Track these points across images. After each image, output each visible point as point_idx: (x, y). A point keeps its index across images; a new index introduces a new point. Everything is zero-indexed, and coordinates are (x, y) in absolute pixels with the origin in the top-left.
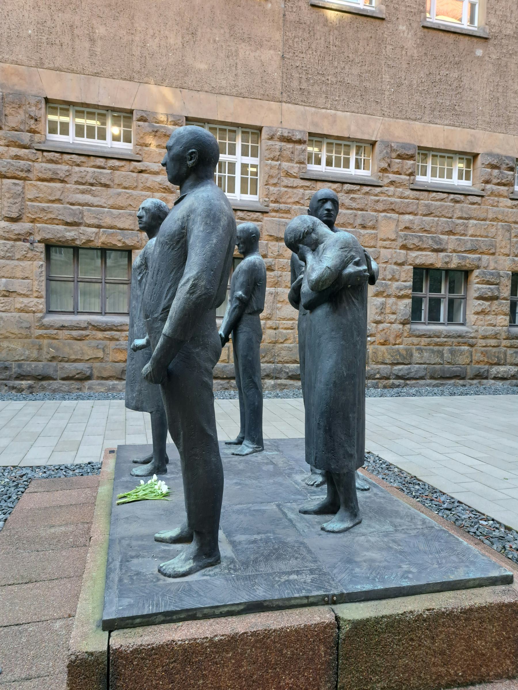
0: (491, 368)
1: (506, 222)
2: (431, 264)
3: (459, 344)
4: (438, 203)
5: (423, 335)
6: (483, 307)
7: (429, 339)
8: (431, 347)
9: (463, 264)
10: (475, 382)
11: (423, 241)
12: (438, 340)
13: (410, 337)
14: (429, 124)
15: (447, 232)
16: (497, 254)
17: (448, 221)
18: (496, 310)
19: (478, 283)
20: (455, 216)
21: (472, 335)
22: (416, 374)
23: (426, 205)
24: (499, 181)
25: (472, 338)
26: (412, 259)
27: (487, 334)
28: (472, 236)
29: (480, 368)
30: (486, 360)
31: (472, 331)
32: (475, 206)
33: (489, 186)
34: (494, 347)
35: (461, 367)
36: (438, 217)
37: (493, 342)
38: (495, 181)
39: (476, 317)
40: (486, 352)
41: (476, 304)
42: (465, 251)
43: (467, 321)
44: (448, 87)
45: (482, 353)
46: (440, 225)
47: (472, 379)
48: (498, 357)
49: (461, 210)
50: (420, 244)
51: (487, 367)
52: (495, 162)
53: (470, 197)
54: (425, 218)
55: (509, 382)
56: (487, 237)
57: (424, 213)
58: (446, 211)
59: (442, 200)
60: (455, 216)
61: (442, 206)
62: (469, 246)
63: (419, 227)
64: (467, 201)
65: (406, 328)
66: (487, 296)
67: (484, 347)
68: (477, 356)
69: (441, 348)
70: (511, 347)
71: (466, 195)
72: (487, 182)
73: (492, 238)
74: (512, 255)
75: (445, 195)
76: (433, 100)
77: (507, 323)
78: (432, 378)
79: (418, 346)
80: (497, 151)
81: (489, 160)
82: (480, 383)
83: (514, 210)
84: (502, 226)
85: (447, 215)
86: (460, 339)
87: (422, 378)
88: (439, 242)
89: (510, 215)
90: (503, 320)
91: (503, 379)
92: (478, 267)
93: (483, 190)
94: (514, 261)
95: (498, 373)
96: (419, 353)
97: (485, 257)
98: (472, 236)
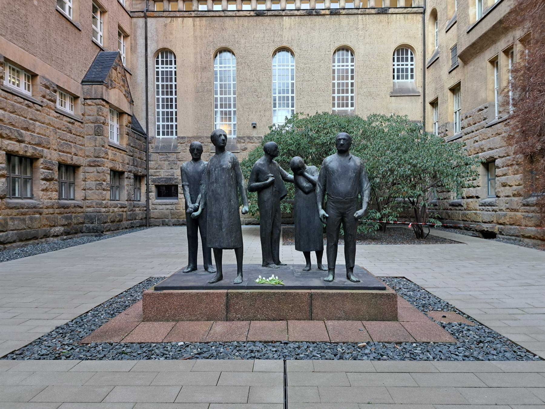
0: (51, 229)
1: (54, 127)
2: (17, 152)
3: (35, 213)
4: (18, 105)
5: (14, 207)
6: (47, 186)
7: (18, 210)
8: (19, 216)
9: (35, 153)
10: (43, 240)
11: (12, 133)
12: (23, 210)
13: (6, 209)
14: (10, 42)
15: (25, 128)
16: (51, 148)
17: (25, 120)
18: (53, 188)
19: (42, 168)
20: (28, 117)
21: (41, 206)
22: (11, 239)
23: (12, 105)
24: (50, 98)
25: (41, 208)
26: (6, 146)
27: (49, 205)
28: (38, 133)
29: (46, 230)
30: (49, 224)
31: (40, 203)
32: (38, 112)
33: (45, 100)
34: (52, 214)
35: (36, 230)
36: (19, 115)
37: (51, 211)
38: (48, 97)
39: (42, 193)
40: (48, 217)
41: (43, 183)
42: (35, 144)
43: (35, 195)
44: (20, 19)
45: (46, 219)
46: (21, 122)
47: (41, 238)
48: (54, 221)
49: (32, 114)
50: (10, 134)
51: (49, 228)
52: (48, 84)
53: (36, 105)
54: (11, 115)
55: (59, 238)
56: (45, 136)
57: (11, 110)
58: (23, 112)
59: (20, 103)
60: (28, 117)
61: (21, 108)
62: (37, 141)
63: (9, 121)
64: (34, 108)
65: (3, 202)
66: (48, 178)
67: (47, 214)
68: (45, 222)
69: (24, 217)
70: (60, 213)
71: (34, 103)
72: (44, 97)
73: (48, 137)
74: (58, 150)
75: (22, 100)
76: (12, 24)
77: (57, 197)
78: (21, 241)
79: (11, 216)
80: (47, 76)
81: (45, 82)
82: (46, 240)
83: (57, 120)
84: (53, 129)
85: (24, 116)
86: (34, 210)
87: (14, 242)
88: (21, 135)
89: (56, 123)
90: (55, 195)
91: (57, 236)
92: (42, 157)
93: (42, 102)
94: (59, 154)
95: (55, 232)
96: (12, 222)
97: (45, 150)
98: (38, 133)
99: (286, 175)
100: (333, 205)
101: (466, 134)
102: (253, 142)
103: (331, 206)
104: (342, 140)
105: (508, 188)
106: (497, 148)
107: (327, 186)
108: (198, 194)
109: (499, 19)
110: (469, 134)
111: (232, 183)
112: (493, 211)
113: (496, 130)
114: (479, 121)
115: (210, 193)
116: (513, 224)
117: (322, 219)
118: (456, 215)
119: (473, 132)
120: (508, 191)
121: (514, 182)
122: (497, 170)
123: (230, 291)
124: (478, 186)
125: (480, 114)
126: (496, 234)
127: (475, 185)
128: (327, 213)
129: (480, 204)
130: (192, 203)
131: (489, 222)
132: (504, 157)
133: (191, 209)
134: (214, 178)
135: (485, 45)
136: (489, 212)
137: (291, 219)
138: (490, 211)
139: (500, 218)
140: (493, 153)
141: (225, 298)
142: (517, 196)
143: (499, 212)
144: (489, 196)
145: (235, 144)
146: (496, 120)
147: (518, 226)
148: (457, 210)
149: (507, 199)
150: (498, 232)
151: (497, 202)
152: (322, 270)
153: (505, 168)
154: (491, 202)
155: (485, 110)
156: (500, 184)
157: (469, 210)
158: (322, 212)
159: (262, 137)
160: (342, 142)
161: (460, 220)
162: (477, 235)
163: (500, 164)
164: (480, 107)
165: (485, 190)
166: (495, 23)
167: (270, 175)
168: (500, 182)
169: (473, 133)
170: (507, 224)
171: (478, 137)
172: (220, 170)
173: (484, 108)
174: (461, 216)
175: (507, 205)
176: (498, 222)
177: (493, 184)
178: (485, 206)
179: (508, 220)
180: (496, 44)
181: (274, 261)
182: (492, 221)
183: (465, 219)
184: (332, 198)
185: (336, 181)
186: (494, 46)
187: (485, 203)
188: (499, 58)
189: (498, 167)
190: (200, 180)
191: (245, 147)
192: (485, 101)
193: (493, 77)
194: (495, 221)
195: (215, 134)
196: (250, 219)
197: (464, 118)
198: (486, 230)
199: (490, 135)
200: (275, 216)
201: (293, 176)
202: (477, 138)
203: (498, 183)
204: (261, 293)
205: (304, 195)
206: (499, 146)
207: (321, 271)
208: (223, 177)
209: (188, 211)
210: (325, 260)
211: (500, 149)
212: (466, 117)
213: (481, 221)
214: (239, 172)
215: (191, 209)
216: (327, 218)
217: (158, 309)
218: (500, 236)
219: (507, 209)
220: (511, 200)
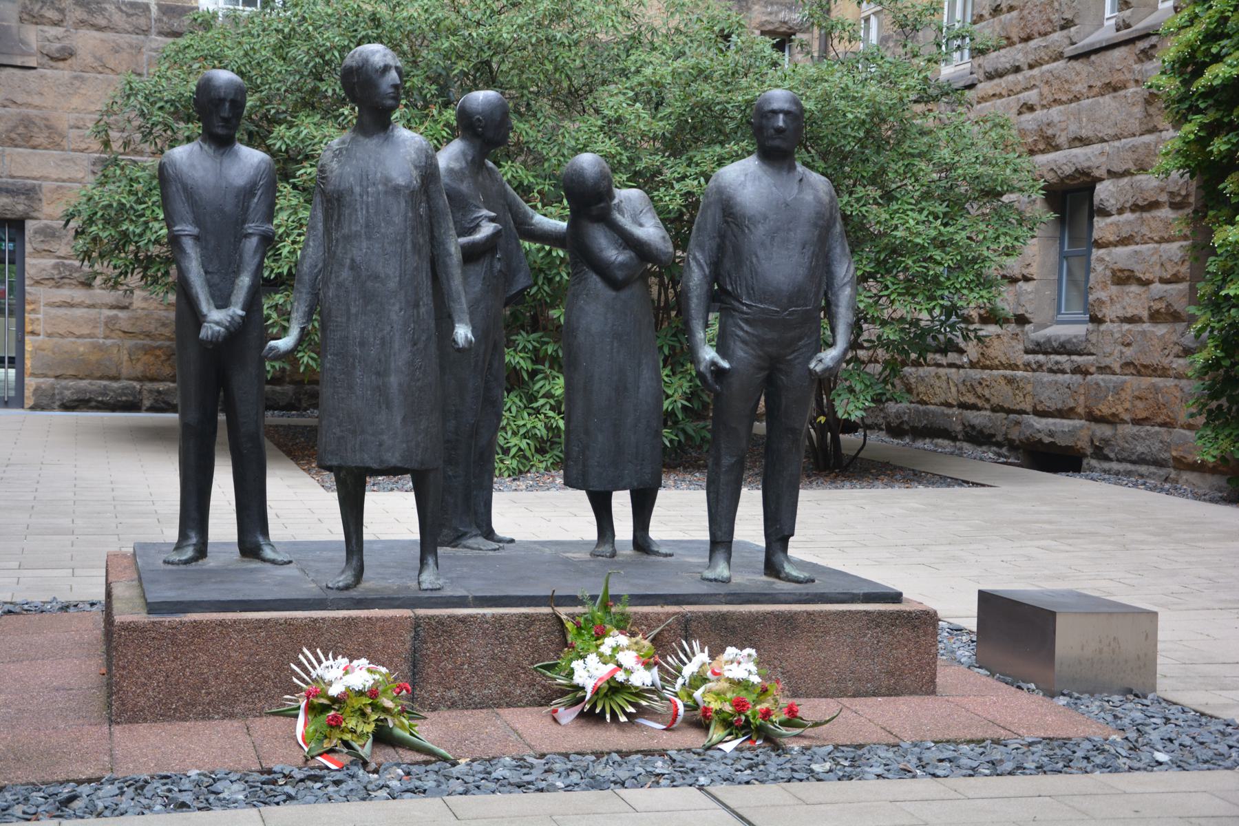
99: (525, 214)
101: (990, 77)
102: (103, 23)
103: (741, 333)
104: (781, 116)
105: (1134, 288)
106: (1103, 141)
107: (728, 264)
108: (237, 273)
110: (1001, 75)
111: (421, 241)
113: (1106, 70)
114: (1042, 29)
115: (345, 274)
116: (1146, 419)
117: (709, 376)
118: (938, 383)
119: (1017, 69)
120: (1134, 300)
121: (1157, 268)
122: (1099, 222)
123: (421, 612)
124: (1027, 279)
126: (1085, 456)
127: (1017, 272)
128: (724, 356)
130: (218, 307)
132: (1126, 173)
133: (217, 328)
134: (362, 221)
136: (1060, 377)
137: (278, 388)
138: (1063, 372)
140: (1089, 159)
141: (408, 637)
142: (1165, 321)
143: (1099, 377)
145: (14, 23)
146: (1107, 32)
147: (1161, 425)
148: (939, 365)
149: (1129, 331)
150: (1089, 451)
151: (1093, 338)
152: (657, 553)
153: (1128, 216)
154: (1069, 341)
156: (1108, 273)
157: (984, 367)
158: (708, 354)
159: (146, 8)
160: (781, 124)
161: (950, 405)
163: (1113, 201)
165: (1049, 292)
167: (485, 212)
168: (1107, 267)
169: (1020, 76)
170: (1123, 422)
171: (1035, 91)
172: (386, 193)
174: (954, 389)
175: (1128, 352)
177: (1079, 274)
178: (1046, 353)
179: (1127, 405)
181: (479, 527)
182: (1072, 409)
183: (970, 399)
185: (761, 253)
187: (1049, 340)
189: (1105, 213)
190: (244, 222)
191: (66, 43)
194: (1080, 410)
195: (367, 61)
196: (84, 384)
197: (986, 13)
198: (1047, 440)
199: (1080, 87)
200: (490, 364)
201: (564, 225)
202: (1032, 96)
203: (1100, 268)
204: (526, 616)
205: (610, 293)
206: (1111, 132)
207: (653, 558)
208: (396, 220)
209: (206, 332)
210: (624, 528)
211: (1117, 143)
212: (996, 11)
213: (1029, 408)
214: (441, 203)
215: (217, 328)
216: (719, 372)
217: (173, 680)
219: (1128, 364)
220: (1144, 333)
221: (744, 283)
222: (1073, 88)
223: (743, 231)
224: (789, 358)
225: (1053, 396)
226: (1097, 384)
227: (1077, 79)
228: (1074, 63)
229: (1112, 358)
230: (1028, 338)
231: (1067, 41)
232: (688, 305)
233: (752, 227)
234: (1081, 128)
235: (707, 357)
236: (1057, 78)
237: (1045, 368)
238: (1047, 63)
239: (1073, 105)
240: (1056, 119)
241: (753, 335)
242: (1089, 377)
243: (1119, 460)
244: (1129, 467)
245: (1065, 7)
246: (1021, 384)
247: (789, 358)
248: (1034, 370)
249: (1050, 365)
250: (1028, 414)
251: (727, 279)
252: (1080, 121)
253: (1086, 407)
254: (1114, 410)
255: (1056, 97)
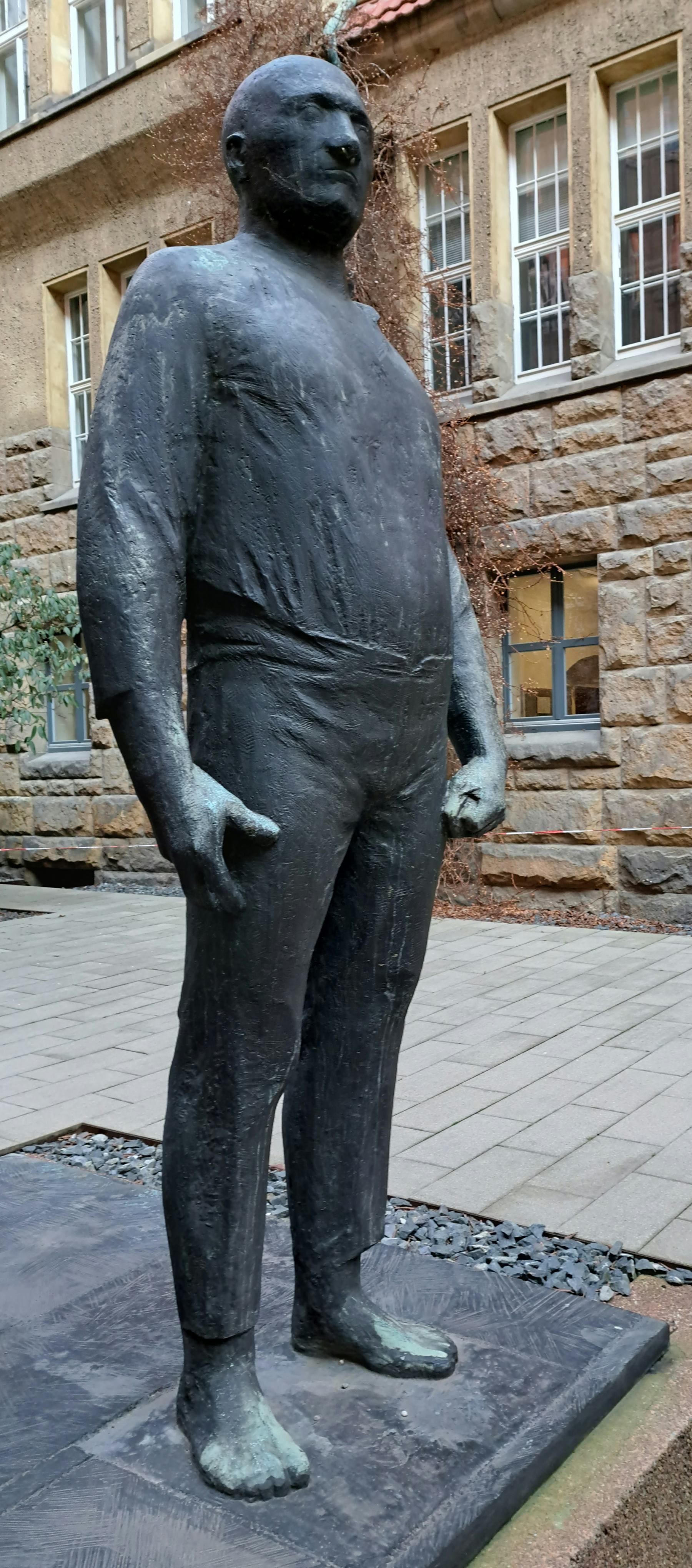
100: (322, 711)
103: (301, 727)
109: (102, 147)
112: (78, 794)
114: (12, 486)
125: (19, 463)
126: (97, 869)
129: (28, 773)
131: (67, 832)
135: (35, 228)
136: (63, 799)
138: (67, 795)
139: (109, 819)
144: (52, 746)
150: (101, 863)
151: (98, 762)
154: (72, 766)
155: (40, 453)
162: (17, 879)
164: (18, 439)
166: (83, 156)
170: (137, 835)
173: (32, 446)
176: (101, 830)
180: (79, 235)
182: (79, 828)
184: (316, 656)
186: (69, 237)
187: (49, 767)
188: (90, 283)
192: (41, 420)
193: (61, 347)
194: (89, 828)
198: (54, 857)
213: (29, 829)
218: (109, 874)
221: (305, 580)
222: (53, 539)
223: (292, 422)
224: (407, 792)
225: (58, 817)
226: (107, 804)
227: (56, 531)
228: (49, 517)
229: (120, 779)
230: (25, 766)
231: (41, 498)
232: (127, 644)
233: (318, 410)
234: (66, 575)
235: (212, 805)
236: (34, 530)
237: (45, 792)
238: (20, 516)
239: (54, 554)
240: (38, 566)
241: (339, 731)
242: (96, 798)
243: (134, 870)
244: (147, 875)
245: (35, 467)
246: (20, 808)
247: (407, 792)
248: (33, 795)
249: (51, 790)
250: (29, 834)
251: (245, 570)
252: (64, 568)
253: (96, 825)
254: (127, 826)
255: (34, 547)
